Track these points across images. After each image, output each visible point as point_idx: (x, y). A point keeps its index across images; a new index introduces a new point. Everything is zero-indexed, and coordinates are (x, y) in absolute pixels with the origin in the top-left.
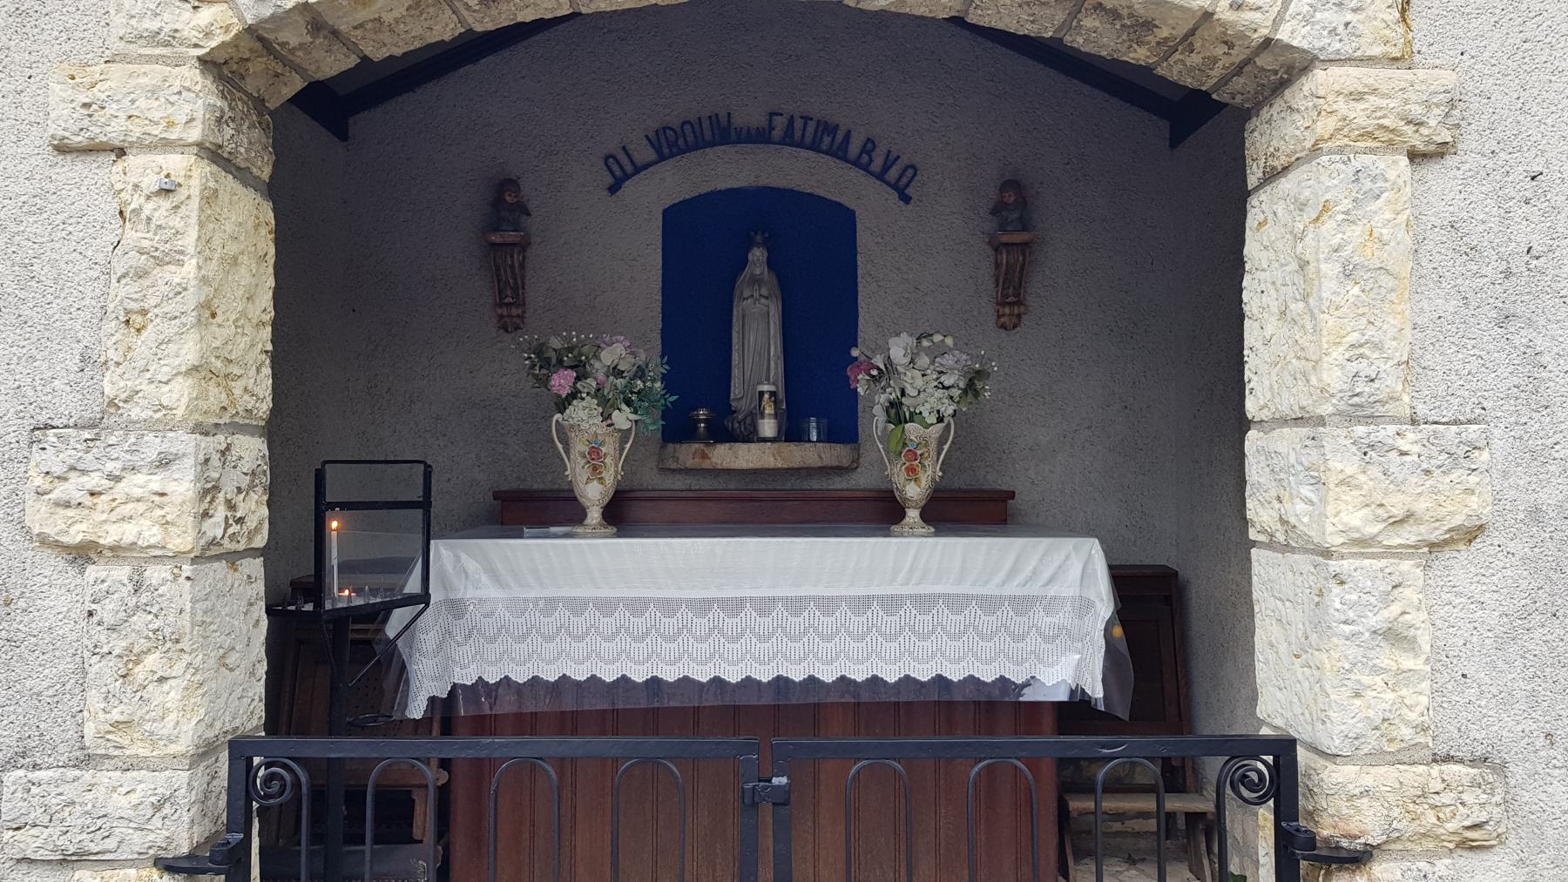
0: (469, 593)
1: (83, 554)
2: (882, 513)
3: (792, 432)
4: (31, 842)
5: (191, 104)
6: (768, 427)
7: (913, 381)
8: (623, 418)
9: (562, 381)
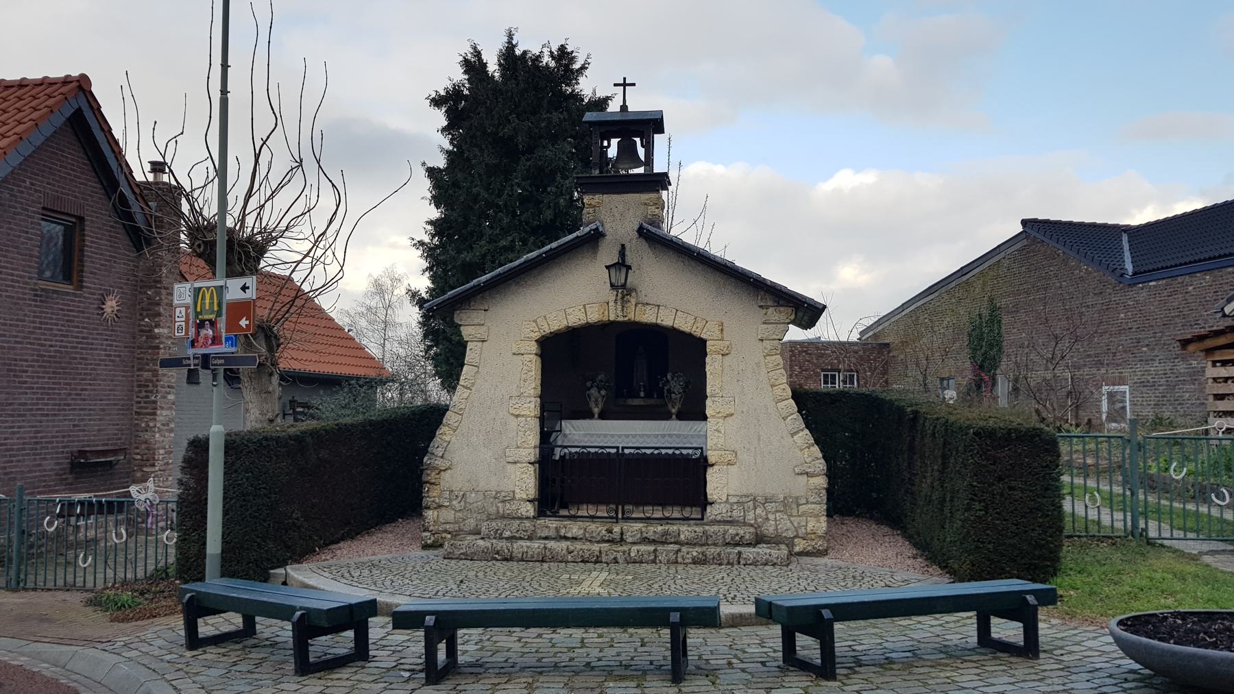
0: (567, 432)
1: (517, 416)
2: (667, 416)
3: (649, 395)
4: (510, 460)
5: (534, 347)
6: (642, 394)
7: (672, 383)
8: (603, 392)
9: (589, 384)
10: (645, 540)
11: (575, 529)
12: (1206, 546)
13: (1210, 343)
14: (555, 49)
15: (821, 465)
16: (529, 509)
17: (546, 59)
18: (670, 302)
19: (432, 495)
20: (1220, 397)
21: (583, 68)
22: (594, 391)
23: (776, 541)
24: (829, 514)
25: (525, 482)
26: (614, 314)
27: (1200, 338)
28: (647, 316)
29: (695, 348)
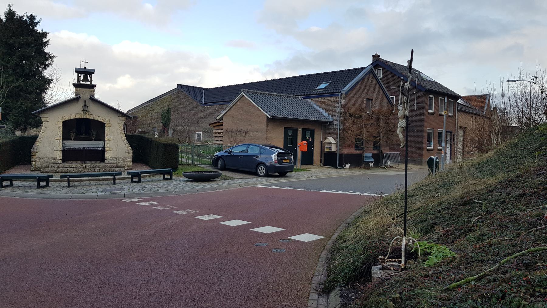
2: (92, 140)
3: (85, 135)
10: (91, 168)
11: (74, 165)
12: (205, 166)
13: (215, 125)
14: (29, 15)
15: (131, 151)
16: (61, 161)
17: (25, 18)
18: (96, 114)
19: (34, 158)
20: (216, 137)
21: (39, 22)
22: (72, 134)
23: (121, 167)
24: (133, 162)
25: (59, 155)
26: (83, 116)
27: (213, 124)
28: (91, 117)
29: (102, 125)
